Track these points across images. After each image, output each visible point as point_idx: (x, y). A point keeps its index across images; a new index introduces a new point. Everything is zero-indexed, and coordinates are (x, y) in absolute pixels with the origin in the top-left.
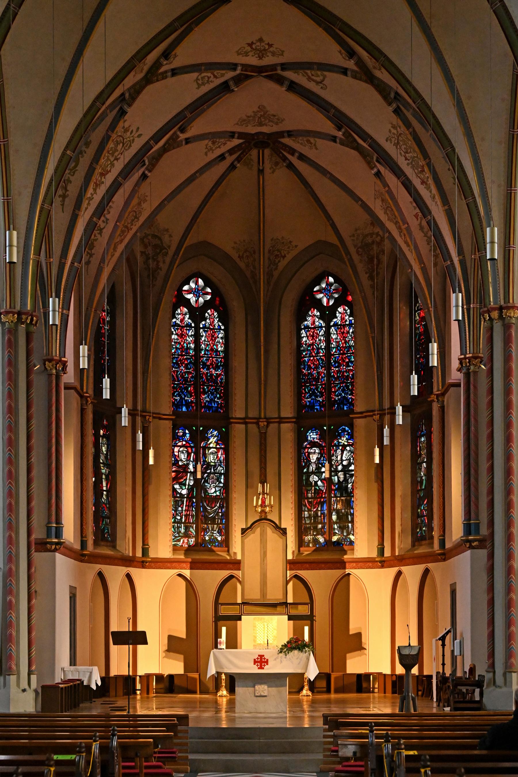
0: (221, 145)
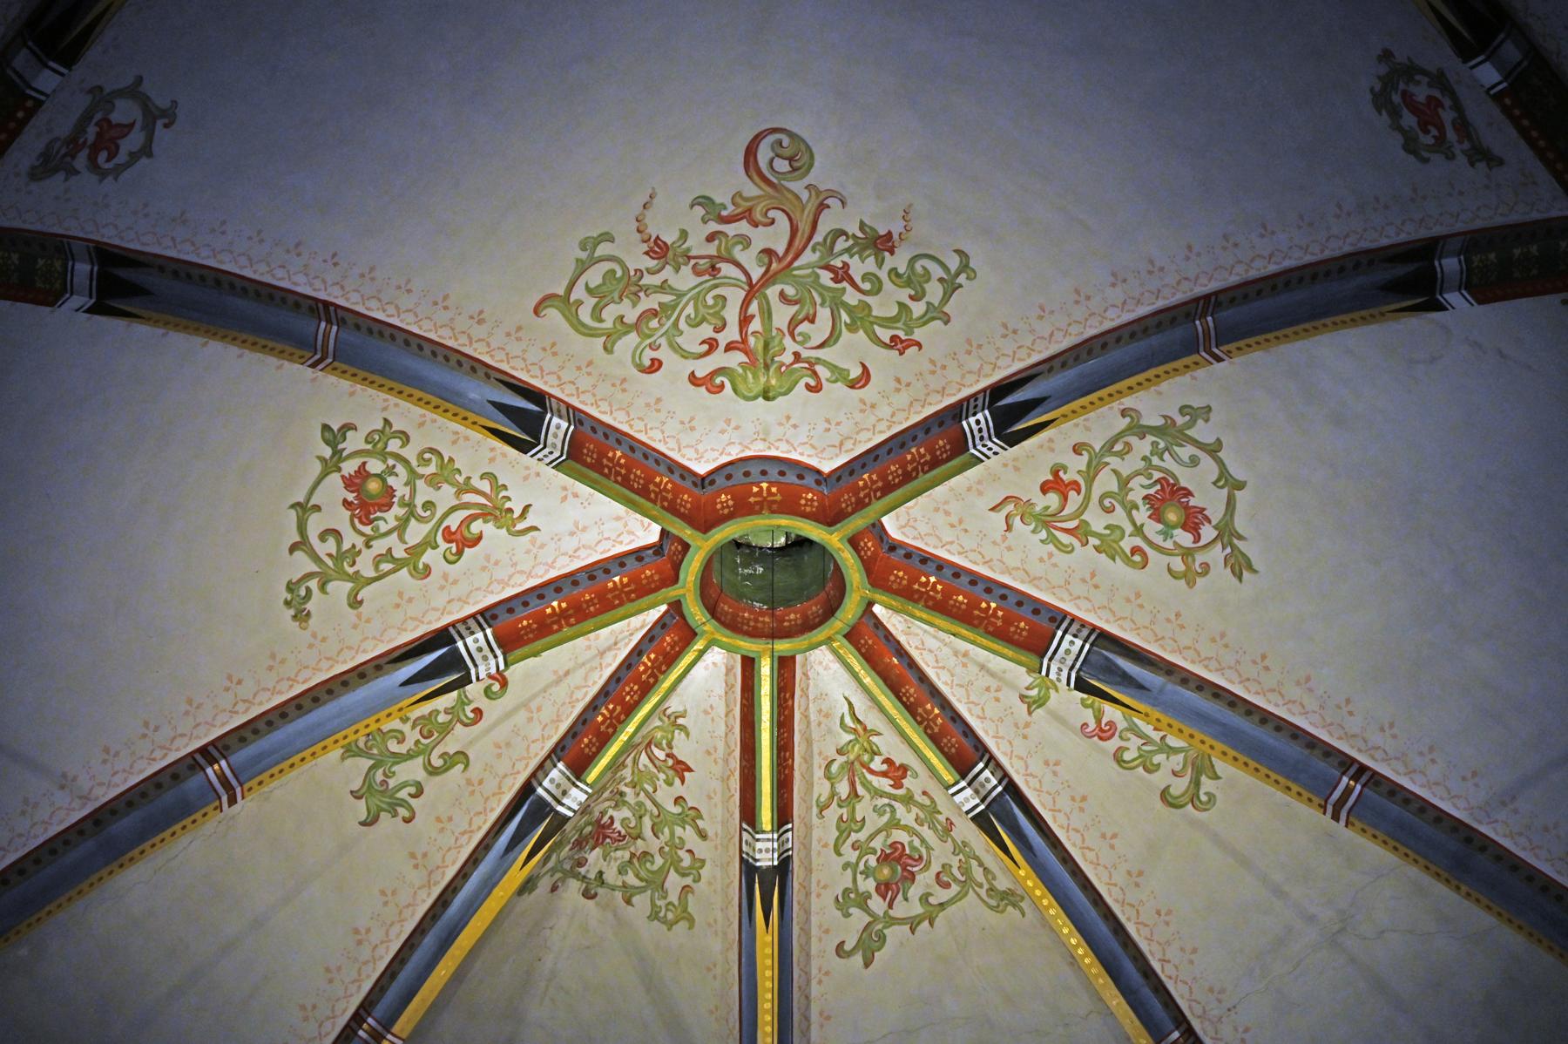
0: (429, 543)
